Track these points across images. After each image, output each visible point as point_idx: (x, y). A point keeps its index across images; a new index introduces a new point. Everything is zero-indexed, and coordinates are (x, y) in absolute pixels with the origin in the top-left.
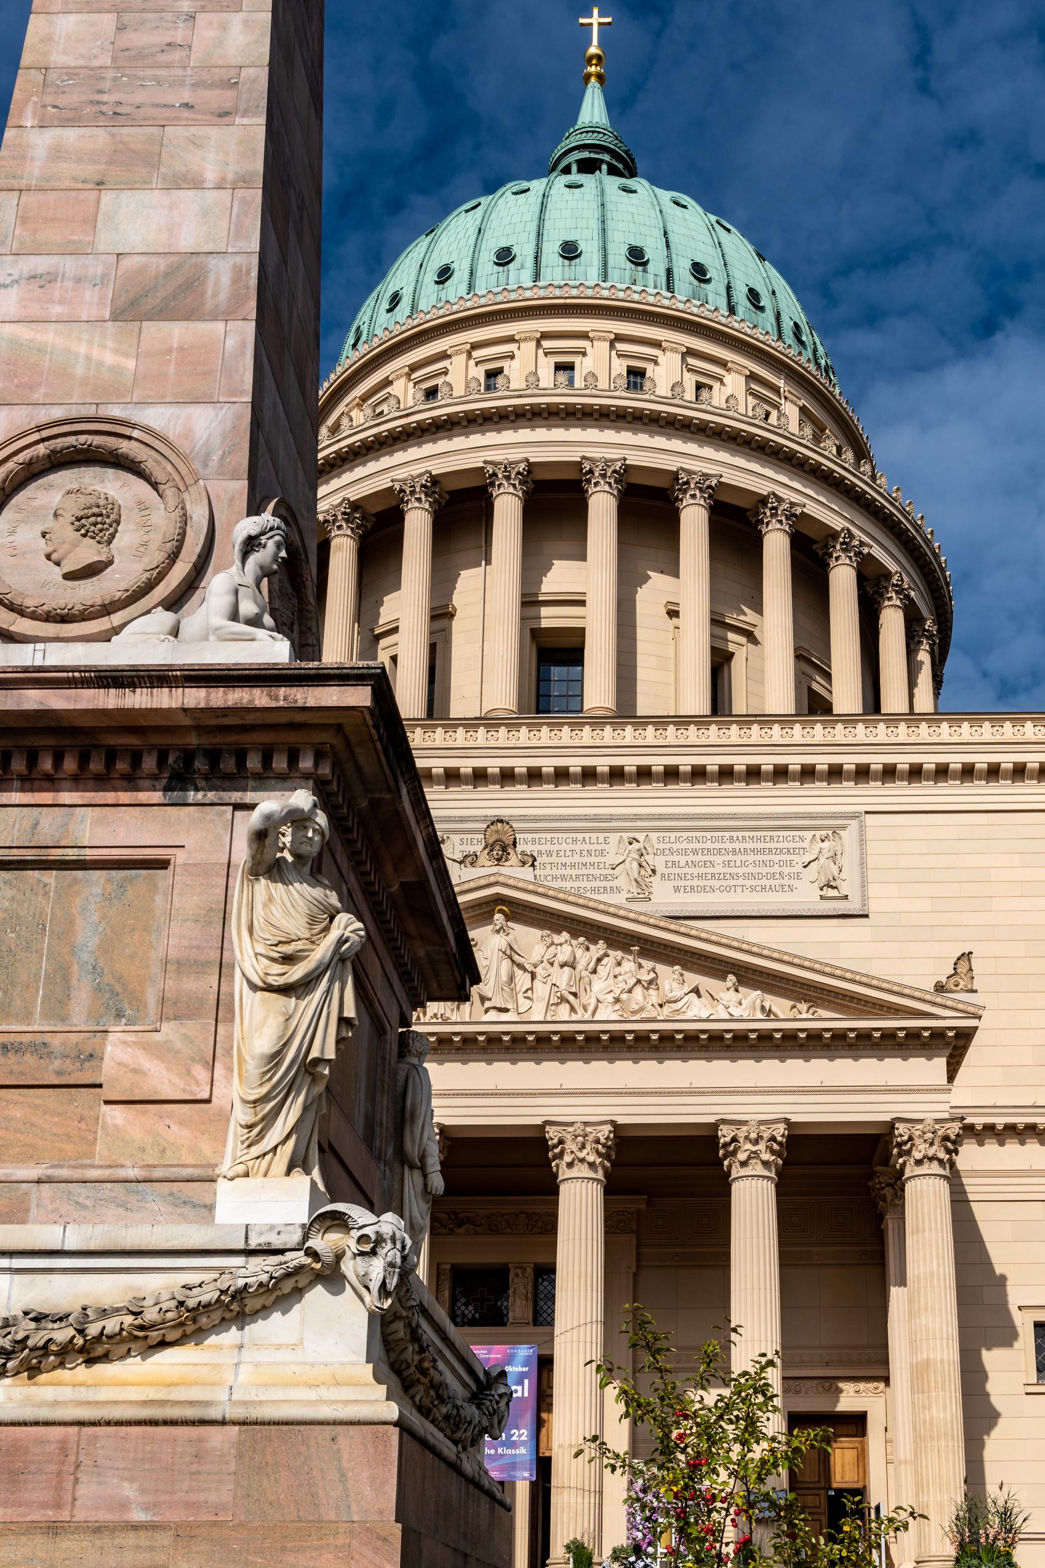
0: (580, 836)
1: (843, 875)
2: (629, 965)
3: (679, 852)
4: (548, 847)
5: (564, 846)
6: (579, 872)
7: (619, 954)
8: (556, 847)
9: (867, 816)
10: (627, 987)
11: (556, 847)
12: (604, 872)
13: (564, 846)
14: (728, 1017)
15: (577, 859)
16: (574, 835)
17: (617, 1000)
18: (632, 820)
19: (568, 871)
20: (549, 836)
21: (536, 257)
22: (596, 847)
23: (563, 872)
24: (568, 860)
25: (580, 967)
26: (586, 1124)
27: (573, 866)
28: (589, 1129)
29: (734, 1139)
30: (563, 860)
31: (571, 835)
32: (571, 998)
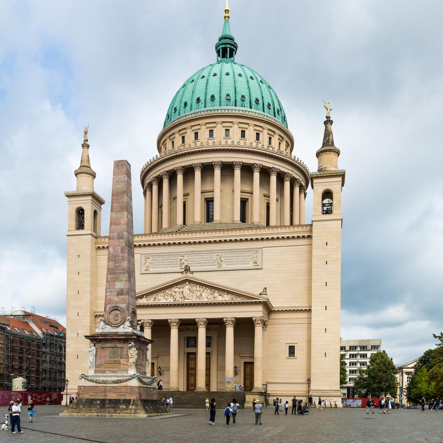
0: (209, 254)
1: (258, 261)
2: (209, 291)
3: (228, 257)
4: (203, 257)
5: (206, 257)
6: (209, 262)
7: (207, 289)
8: (204, 257)
9: (264, 248)
10: (208, 295)
11: (204, 257)
12: (213, 261)
13: (206, 257)
14: (224, 300)
15: (208, 259)
16: (208, 254)
17: (207, 297)
18: (218, 251)
19: (207, 262)
20: (203, 254)
21: (205, 101)
22: (212, 256)
23: (206, 262)
24: (207, 259)
25: (201, 291)
26: (202, 318)
27: (207, 260)
28: (202, 319)
29: (226, 321)
30: (206, 259)
31: (207, 254)
32: (199, 297)
